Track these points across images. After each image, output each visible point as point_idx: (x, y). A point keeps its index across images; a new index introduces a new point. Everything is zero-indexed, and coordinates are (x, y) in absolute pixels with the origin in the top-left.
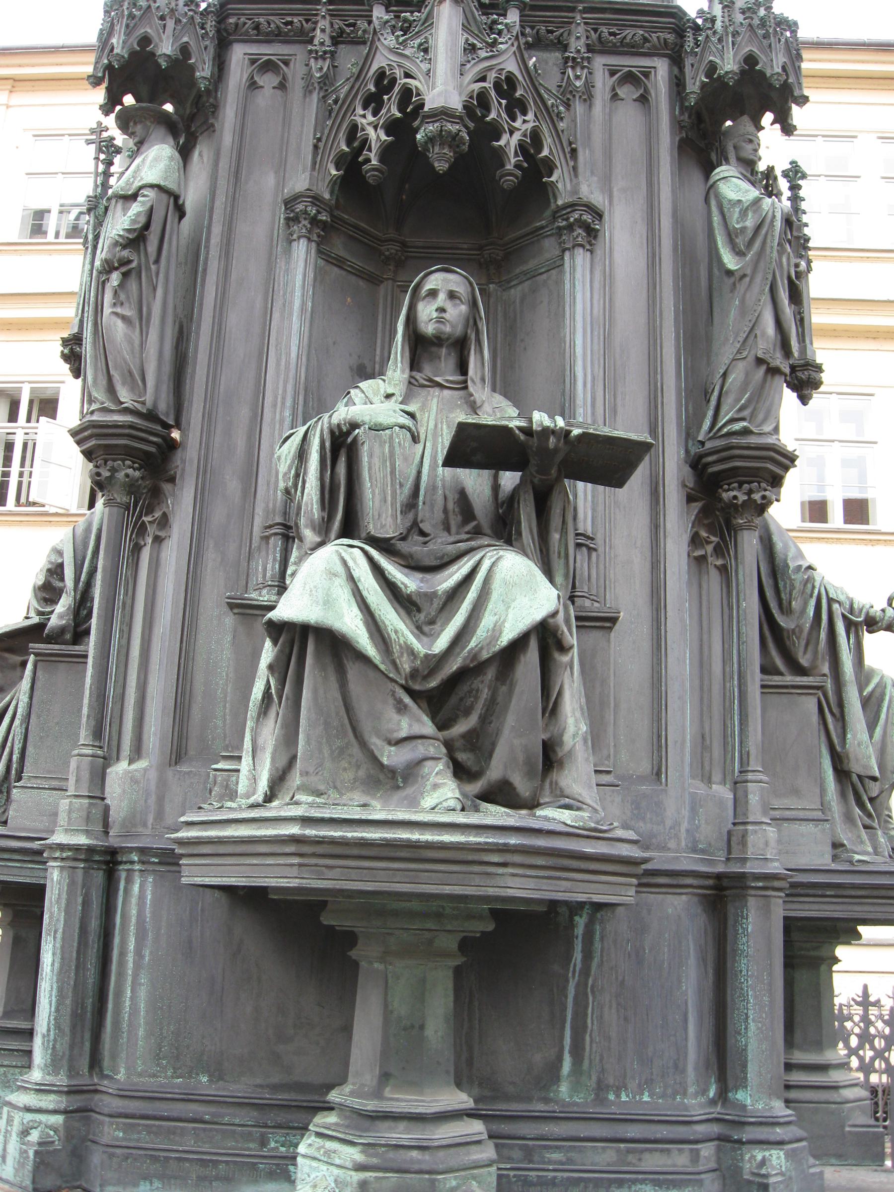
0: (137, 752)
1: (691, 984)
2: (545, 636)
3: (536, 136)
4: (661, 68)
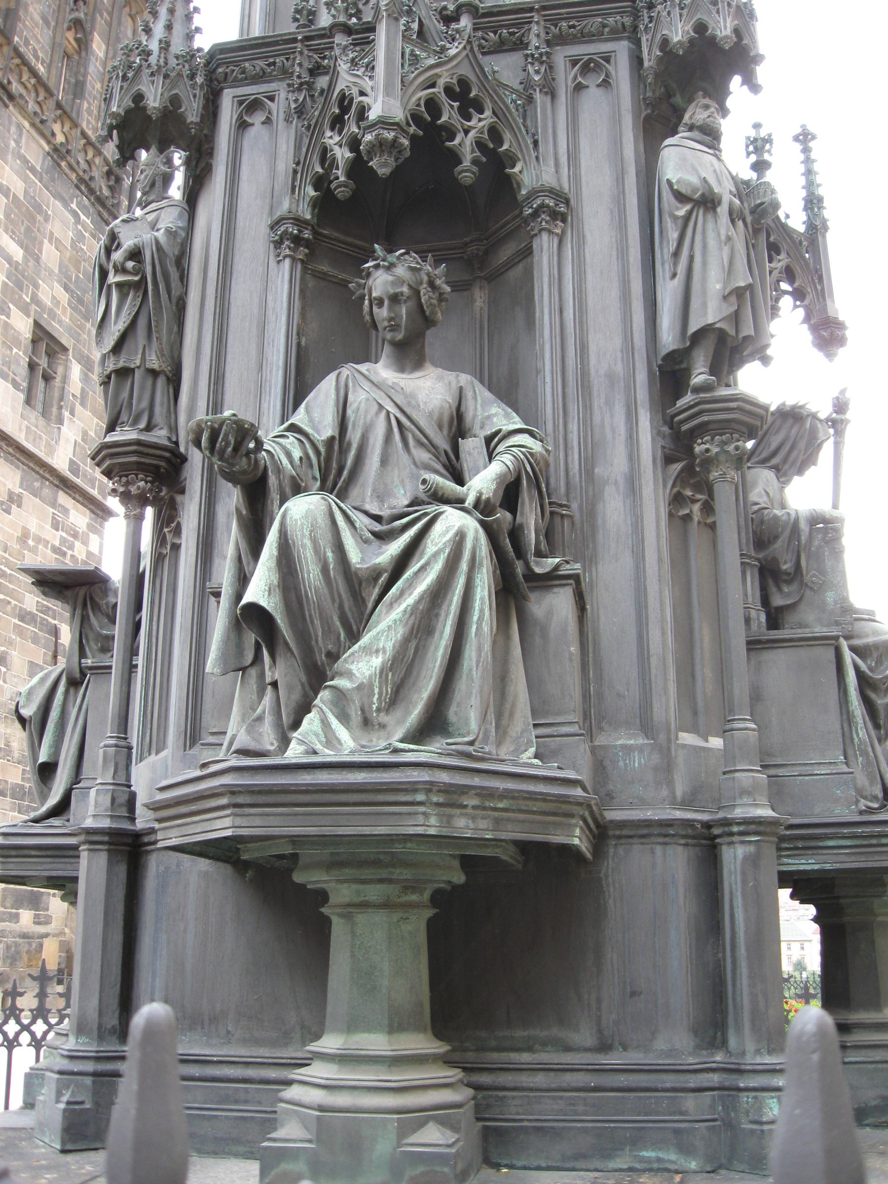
3: (494, 133)
4: (621, 49)
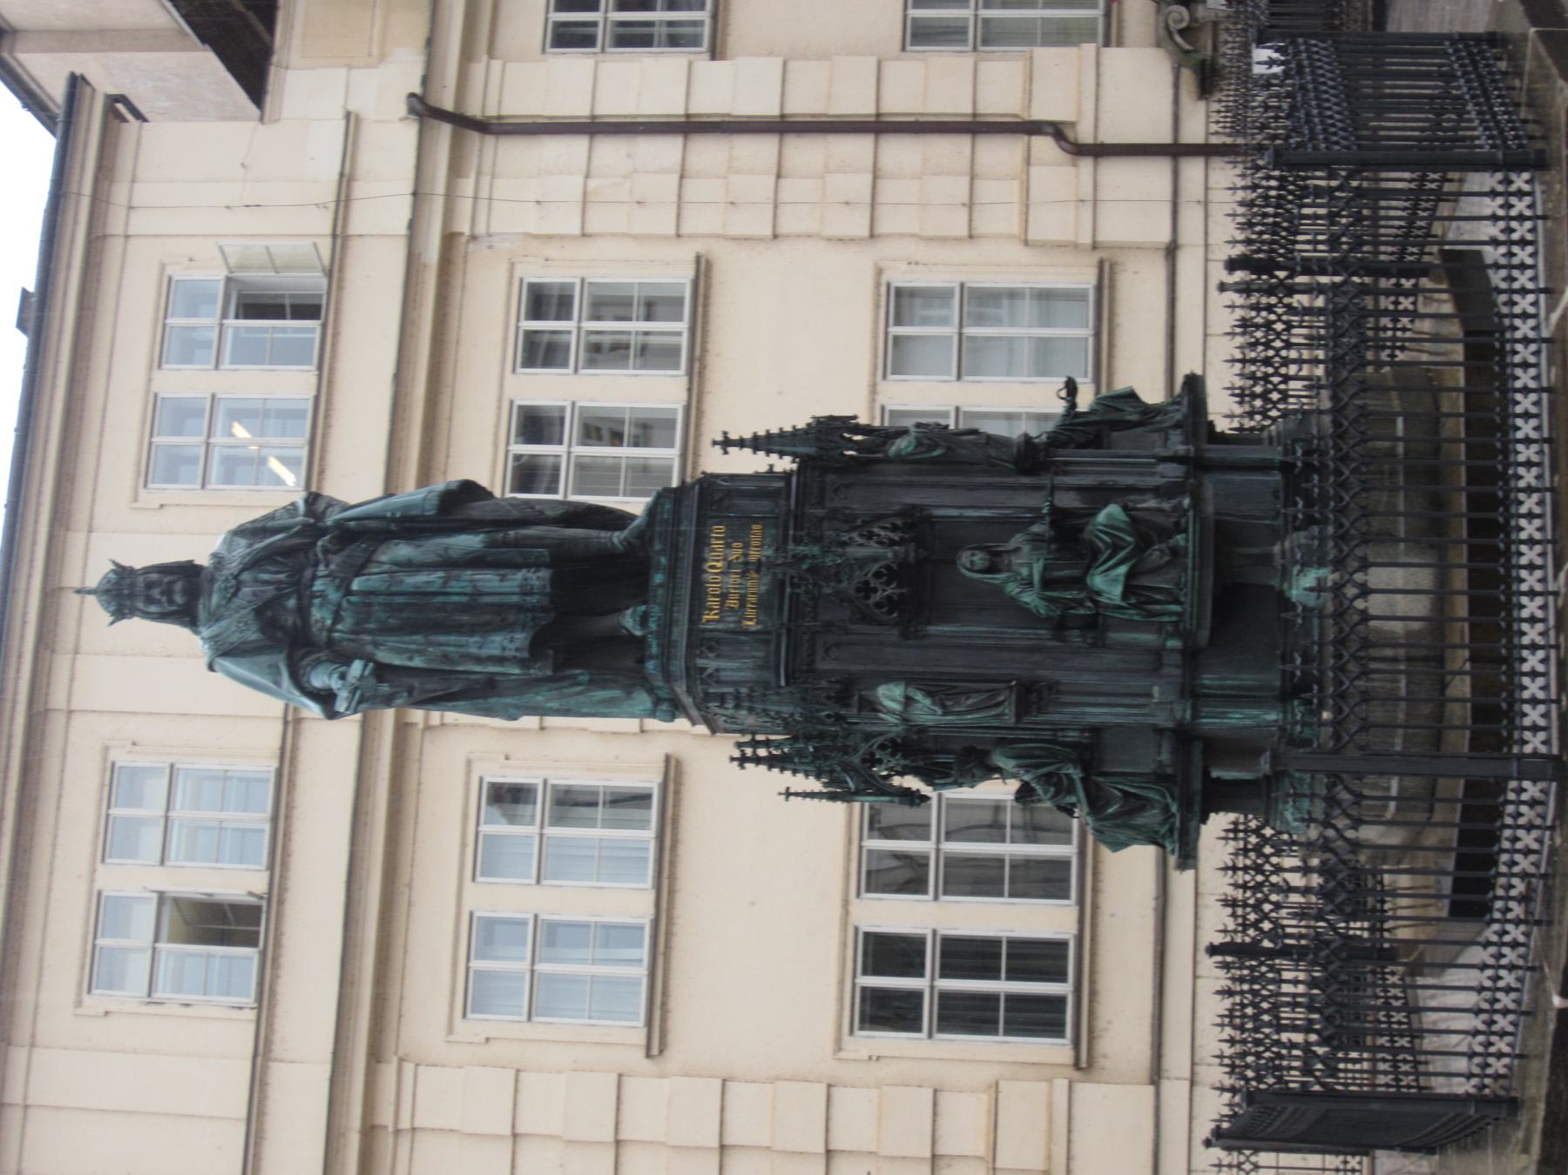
0: (1149, 695)
1: (1237, 477)
2: (1125, 508)
3: (884, 528)
